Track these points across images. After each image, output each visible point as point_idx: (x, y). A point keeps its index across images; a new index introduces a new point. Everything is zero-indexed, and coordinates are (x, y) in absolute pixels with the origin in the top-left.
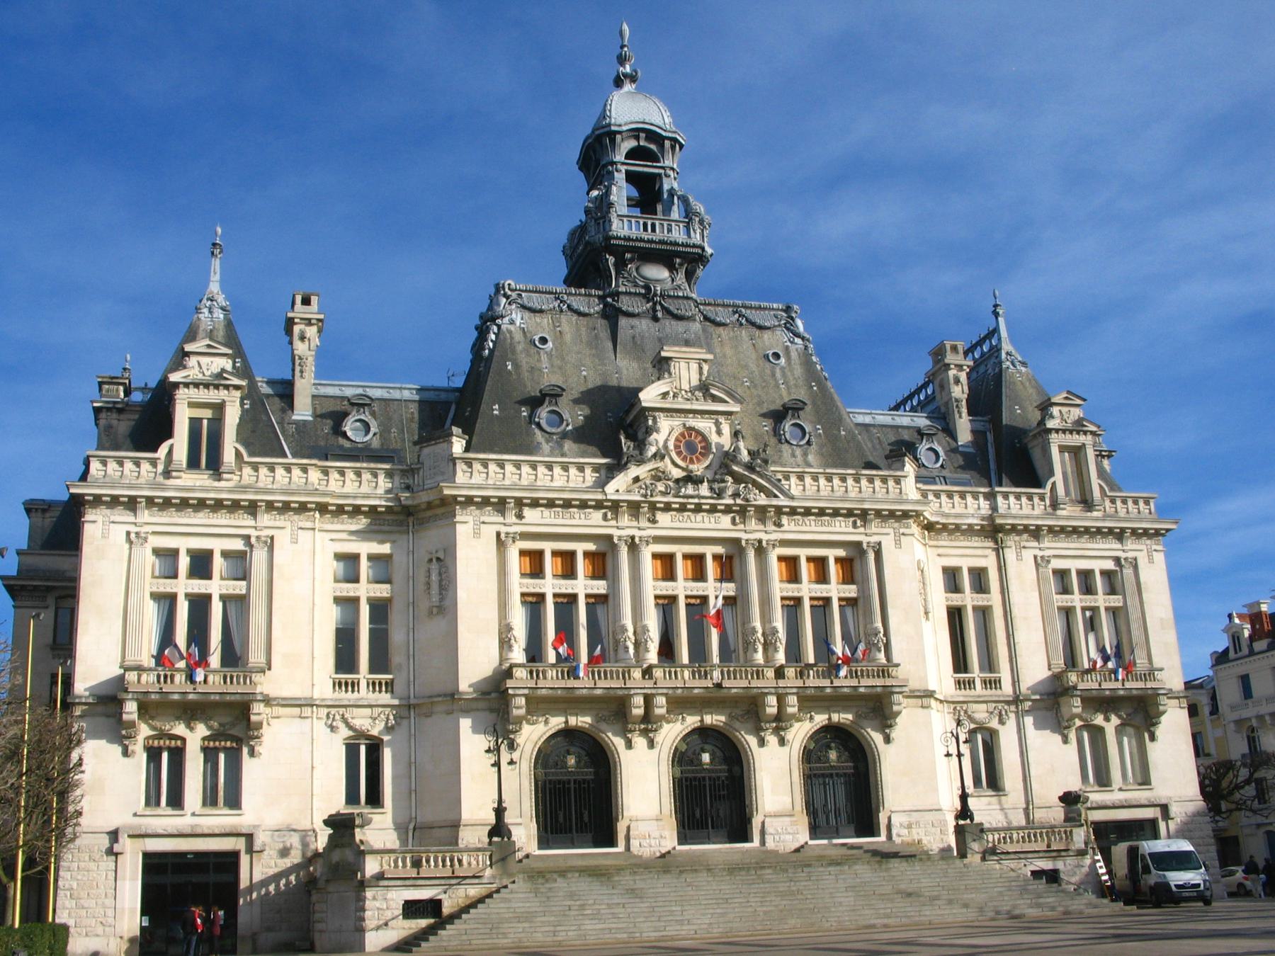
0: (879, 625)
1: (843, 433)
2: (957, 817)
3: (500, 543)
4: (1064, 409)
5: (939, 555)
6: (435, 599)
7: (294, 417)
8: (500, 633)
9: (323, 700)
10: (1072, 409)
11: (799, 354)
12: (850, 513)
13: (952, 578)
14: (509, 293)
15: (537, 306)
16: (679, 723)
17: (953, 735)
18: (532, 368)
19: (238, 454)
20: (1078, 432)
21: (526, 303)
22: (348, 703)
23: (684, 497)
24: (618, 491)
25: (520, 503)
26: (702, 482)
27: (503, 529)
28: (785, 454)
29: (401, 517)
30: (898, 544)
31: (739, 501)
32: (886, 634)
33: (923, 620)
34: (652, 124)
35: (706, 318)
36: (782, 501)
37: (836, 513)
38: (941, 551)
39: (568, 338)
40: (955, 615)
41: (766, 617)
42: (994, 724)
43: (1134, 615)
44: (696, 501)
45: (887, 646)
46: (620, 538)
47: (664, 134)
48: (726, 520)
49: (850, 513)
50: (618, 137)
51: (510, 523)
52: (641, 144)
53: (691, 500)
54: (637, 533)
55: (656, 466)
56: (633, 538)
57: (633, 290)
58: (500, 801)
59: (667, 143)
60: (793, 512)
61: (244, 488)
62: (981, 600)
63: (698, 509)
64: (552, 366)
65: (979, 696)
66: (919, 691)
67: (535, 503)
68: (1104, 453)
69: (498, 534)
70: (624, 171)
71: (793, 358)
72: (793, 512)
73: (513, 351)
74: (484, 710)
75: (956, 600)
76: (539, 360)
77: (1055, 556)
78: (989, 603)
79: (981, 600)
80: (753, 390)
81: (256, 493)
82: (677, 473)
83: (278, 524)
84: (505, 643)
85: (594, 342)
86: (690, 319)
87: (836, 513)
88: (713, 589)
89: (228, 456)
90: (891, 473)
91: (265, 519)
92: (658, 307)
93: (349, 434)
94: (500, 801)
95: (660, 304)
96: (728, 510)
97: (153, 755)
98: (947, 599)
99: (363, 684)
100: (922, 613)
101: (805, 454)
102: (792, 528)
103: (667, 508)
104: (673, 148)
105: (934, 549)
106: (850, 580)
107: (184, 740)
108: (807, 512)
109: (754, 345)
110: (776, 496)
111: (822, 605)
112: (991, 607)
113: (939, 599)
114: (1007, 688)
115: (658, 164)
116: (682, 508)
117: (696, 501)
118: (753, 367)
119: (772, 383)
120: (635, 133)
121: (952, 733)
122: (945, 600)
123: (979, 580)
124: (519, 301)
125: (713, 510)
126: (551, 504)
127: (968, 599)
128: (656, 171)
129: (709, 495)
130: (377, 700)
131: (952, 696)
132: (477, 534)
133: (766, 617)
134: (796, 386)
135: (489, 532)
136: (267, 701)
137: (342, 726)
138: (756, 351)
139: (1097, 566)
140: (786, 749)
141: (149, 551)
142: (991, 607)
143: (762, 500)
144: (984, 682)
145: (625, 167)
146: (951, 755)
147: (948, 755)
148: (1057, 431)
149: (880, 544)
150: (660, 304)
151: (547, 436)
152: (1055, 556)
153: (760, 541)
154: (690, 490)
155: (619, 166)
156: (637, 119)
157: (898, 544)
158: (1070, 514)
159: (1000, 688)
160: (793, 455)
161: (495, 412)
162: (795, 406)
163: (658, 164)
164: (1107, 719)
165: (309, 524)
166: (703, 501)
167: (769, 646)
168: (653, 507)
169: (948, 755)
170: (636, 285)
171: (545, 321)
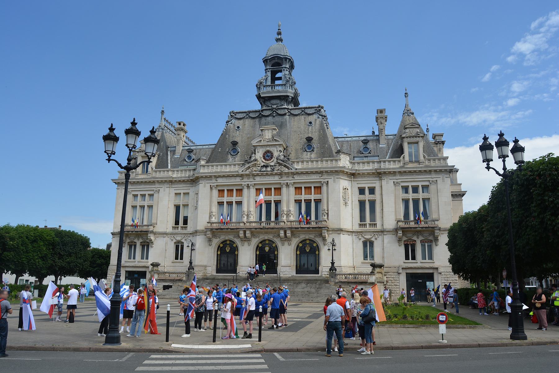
0: (326, 208)
1: (326, 146)
2: (330, 270)
3: (211, 188)
4: (411, 130)
5: (357, 184)
6: (195, 204)
7: (175, 156)
8: (210, 213)
9: (169, 232)
10: (414, 129)
11: (319, 121)
12: (317, 173)
13: (362, 191)
14: (232, 114)
15: (239, 117)
16: (257, 239)
17: (331, 243)
18: (234, 136)
19: (152, 168)
20: (416, 137)
21: (237, 117)
22: (175, 233)
23: (262, 172)
24: (243, 171)
25: (216, 177)
26: (268, 167)
27: (212, 184)
28: (304, 155)
29: (192, 182)
30: (334, 181)
31: (279, 172)
32: (328, 210)
33: (342, 207)
34: (278, 55)
35: (291, 114)
36: (293, 171)
37: (312, 173)
38: (357, 182)
39: (246, 125)
40: (362, 204)
41: (288, 206)
42: (373, 239)
43: (433, 201)
44: (266, 172)
45: (328, 214)
46: (245, 185)
47: (282, 57)
48: (277, 178)
49: (317, 173)
50: (268, 61)
51: (214, 182)
52: (276, 61)
53: (265, 172)
54: (249, 183)
55: (254, 163)
56: (248, 184)
57: (268, 108)
58: (191, 260)
59: (284, 59)
60: (297, 173)
61: (154, 178)
62: (372, 197)
63: (267, 175)
64: (239, 135)
65: (367, 230)
66: (336, 228)
67: (220, 177)
68: (440, 142)
69: (211, 186)
70: (270, 71)
71: (317, 123)
72: (297, 173)
73: (229, 132)
74: (203, 235)
75: (362, 197)
76: (236, 134)
77: (402, 182)
78: (375, 199)
79: (372, 197)
80: (300, 135)
81: (154, 179)
82: (263, 164)
83: (161, 186)
84: (210, 217)
85: (254, 127)
86: (285, 114)
87: (312, 173)
88: (273, 198)
89: (150, 169)
90: (334, 158)
91: (157, 185)
92: (274, 112)
93: (186, 160)
94: (191, 260)
95: (275, 112)
96: (276, 174)
97: (130, 247)
98: (359, 198)
99: (180, 228)
100: (342, 202)
101: (311, 154)
102: (298, 178)
103: (258, 175)
104: (286, 60)
105: (356, 182)
106: (320, 193)
107: (136, 243)
108: (302, 173)
109: (305, 120)
110: (291, 169)
111: (308, 202)
112: (375, 200)
113: (354, 198)
114: (379, 227)
115: (281, 67)
116: (262, 175)
117: (266, 172)
118: (302, 127)
119: (307, 132)
120: (273, 58)
121: (331, 243)
122: (358, 198)
123: (372, 191)
124: (235, 116)
125: (272, 175)
126: (224, 176)
127: (367, 197)
128: (281, 69)
129: (270, 170)
130: (182, 232)
131: (356, 230)
132: (205, 186)
133: (288, 206)
134: (315, 132)
135: (208, 185)
136: (152, 232)
137: (174, 239)
138: (305, 122)
139: (420, 184)
140: (290, 246)
141: (132, 195)
142: (375, 200)
143: (286, 170)
144: (370, 224)
145: (270, 70)
146: (330, 250)
147: (329, 250)
148: (407, 137)
149: (328, 181)
150: (275, 112)
151: (232, 156)
152: (402, 182)
153: (287, 183)
154: (264, 169)
155: (269, 70)
156: (272, 54)
157: (334, 181)
158: (411, 166)
159: (376, 227)
160: (307, 155)
161: (219, 151)
162: (308, 139)
163: (281, 67)
164: (418, 238)
165: (169, 186)
166: (268, 172)
167: (288, 215)
168: (254, 176)
169: (329, 250)
170: (269, 107)
171: (241, 121)
